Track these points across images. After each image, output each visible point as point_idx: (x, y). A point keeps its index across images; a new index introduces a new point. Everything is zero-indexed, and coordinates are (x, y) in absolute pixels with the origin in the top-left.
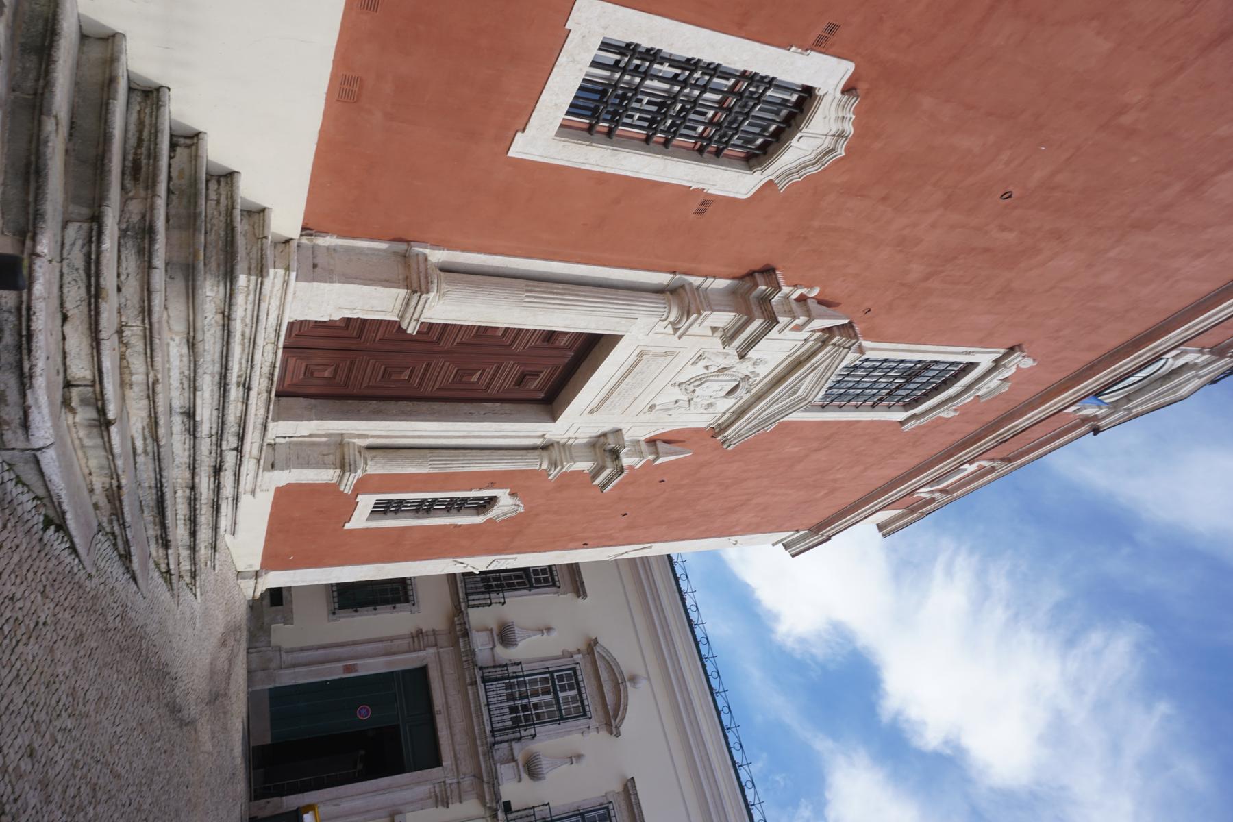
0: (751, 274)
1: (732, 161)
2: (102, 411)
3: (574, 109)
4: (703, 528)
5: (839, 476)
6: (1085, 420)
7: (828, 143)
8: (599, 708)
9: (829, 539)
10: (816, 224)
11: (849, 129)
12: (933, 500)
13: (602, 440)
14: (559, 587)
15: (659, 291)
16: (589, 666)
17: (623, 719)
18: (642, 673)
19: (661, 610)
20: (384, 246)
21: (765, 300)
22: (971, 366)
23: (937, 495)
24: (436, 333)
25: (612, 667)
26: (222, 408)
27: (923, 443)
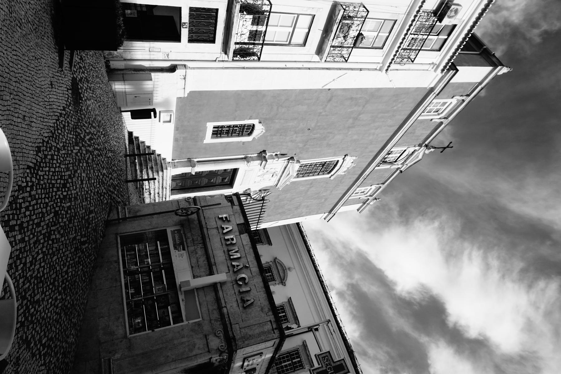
0: (261, 152)
1: (245, 136)
2: (150, 192)
3: (213, 134)
4: (292, 215)
5: (324, 194)
6: (398, 169)
7: (262, 130)
8: (279, 278)
9: (335, 214)
10: (269, 142)
11: (264, 128)
12: (368, 199)
13: (246, 191)
14: (263, 243)
15: (242, 159)
16: (274, 265)
17: (286, 280)
18: (292, 266)
19: (297, 247)
20: (186, 160)
21: (265, 157)
22: (338, 161)
23: (369, 197)
24: (199, 174)
25: (282, 265)
26: (163, 192)
27: (343, 182)
